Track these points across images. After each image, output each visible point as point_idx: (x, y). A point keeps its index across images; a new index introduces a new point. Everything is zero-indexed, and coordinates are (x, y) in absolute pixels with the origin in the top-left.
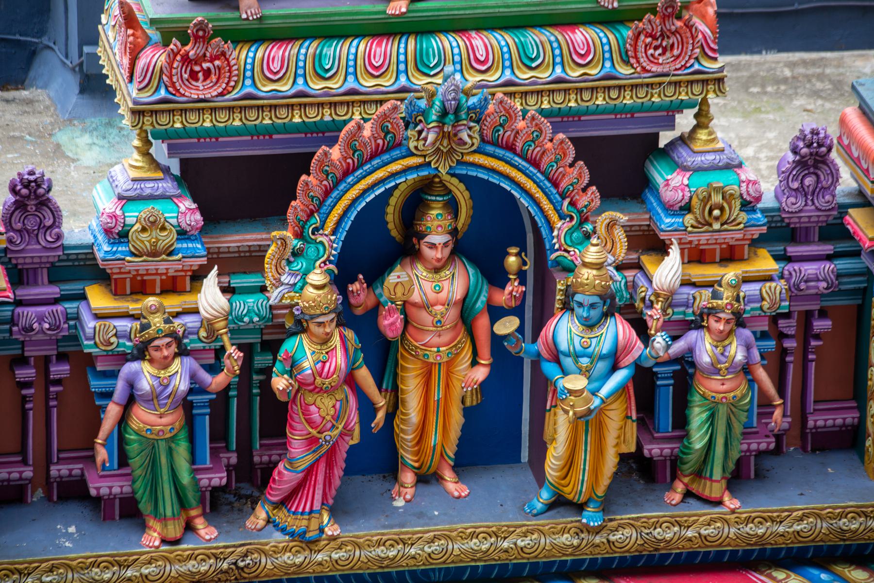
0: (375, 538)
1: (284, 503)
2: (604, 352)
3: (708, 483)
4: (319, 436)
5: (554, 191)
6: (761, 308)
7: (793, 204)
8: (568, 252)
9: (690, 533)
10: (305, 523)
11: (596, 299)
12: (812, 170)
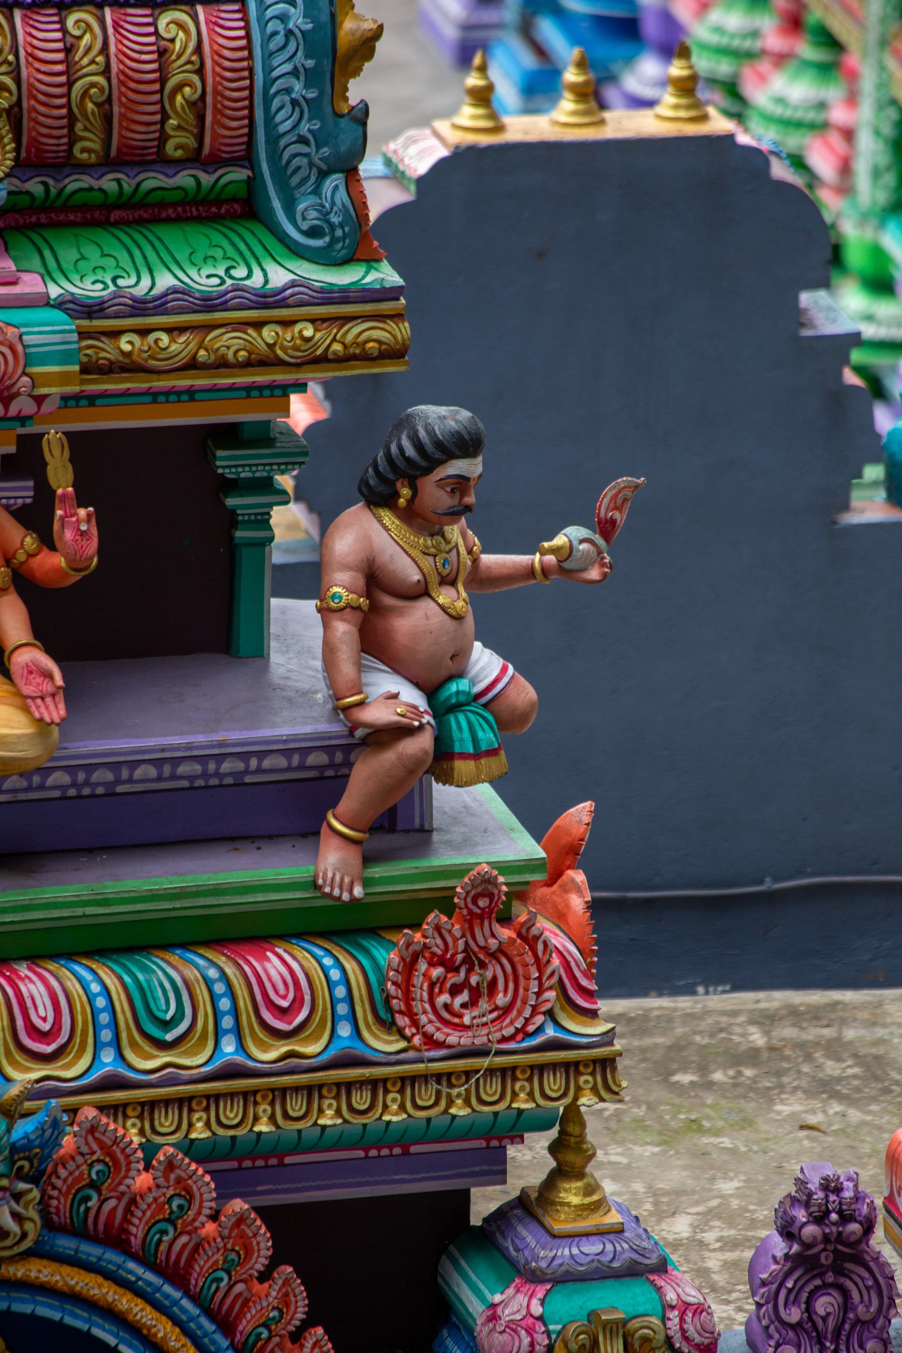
12: (830, 1278)
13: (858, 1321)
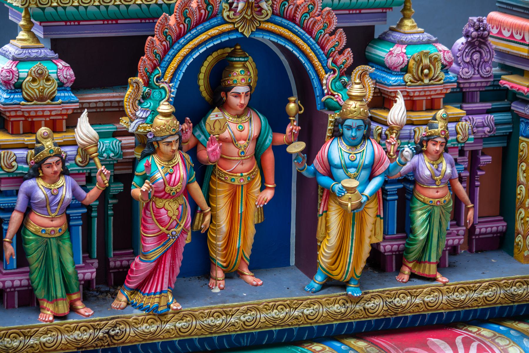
0: (206, 311)
1: (139, 289)
2: (366, 163)
3: (427, 265)
4: (167, 232)
5: (322, 52)
6: (457, 140)
7: (467, 73)
8: (334, 95)
9: (418, 301)
10: (157, 300)
11: (360, 123)
12: (478, 49)
13: (484, 61)
